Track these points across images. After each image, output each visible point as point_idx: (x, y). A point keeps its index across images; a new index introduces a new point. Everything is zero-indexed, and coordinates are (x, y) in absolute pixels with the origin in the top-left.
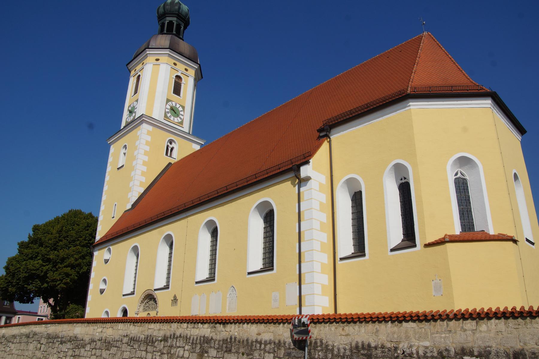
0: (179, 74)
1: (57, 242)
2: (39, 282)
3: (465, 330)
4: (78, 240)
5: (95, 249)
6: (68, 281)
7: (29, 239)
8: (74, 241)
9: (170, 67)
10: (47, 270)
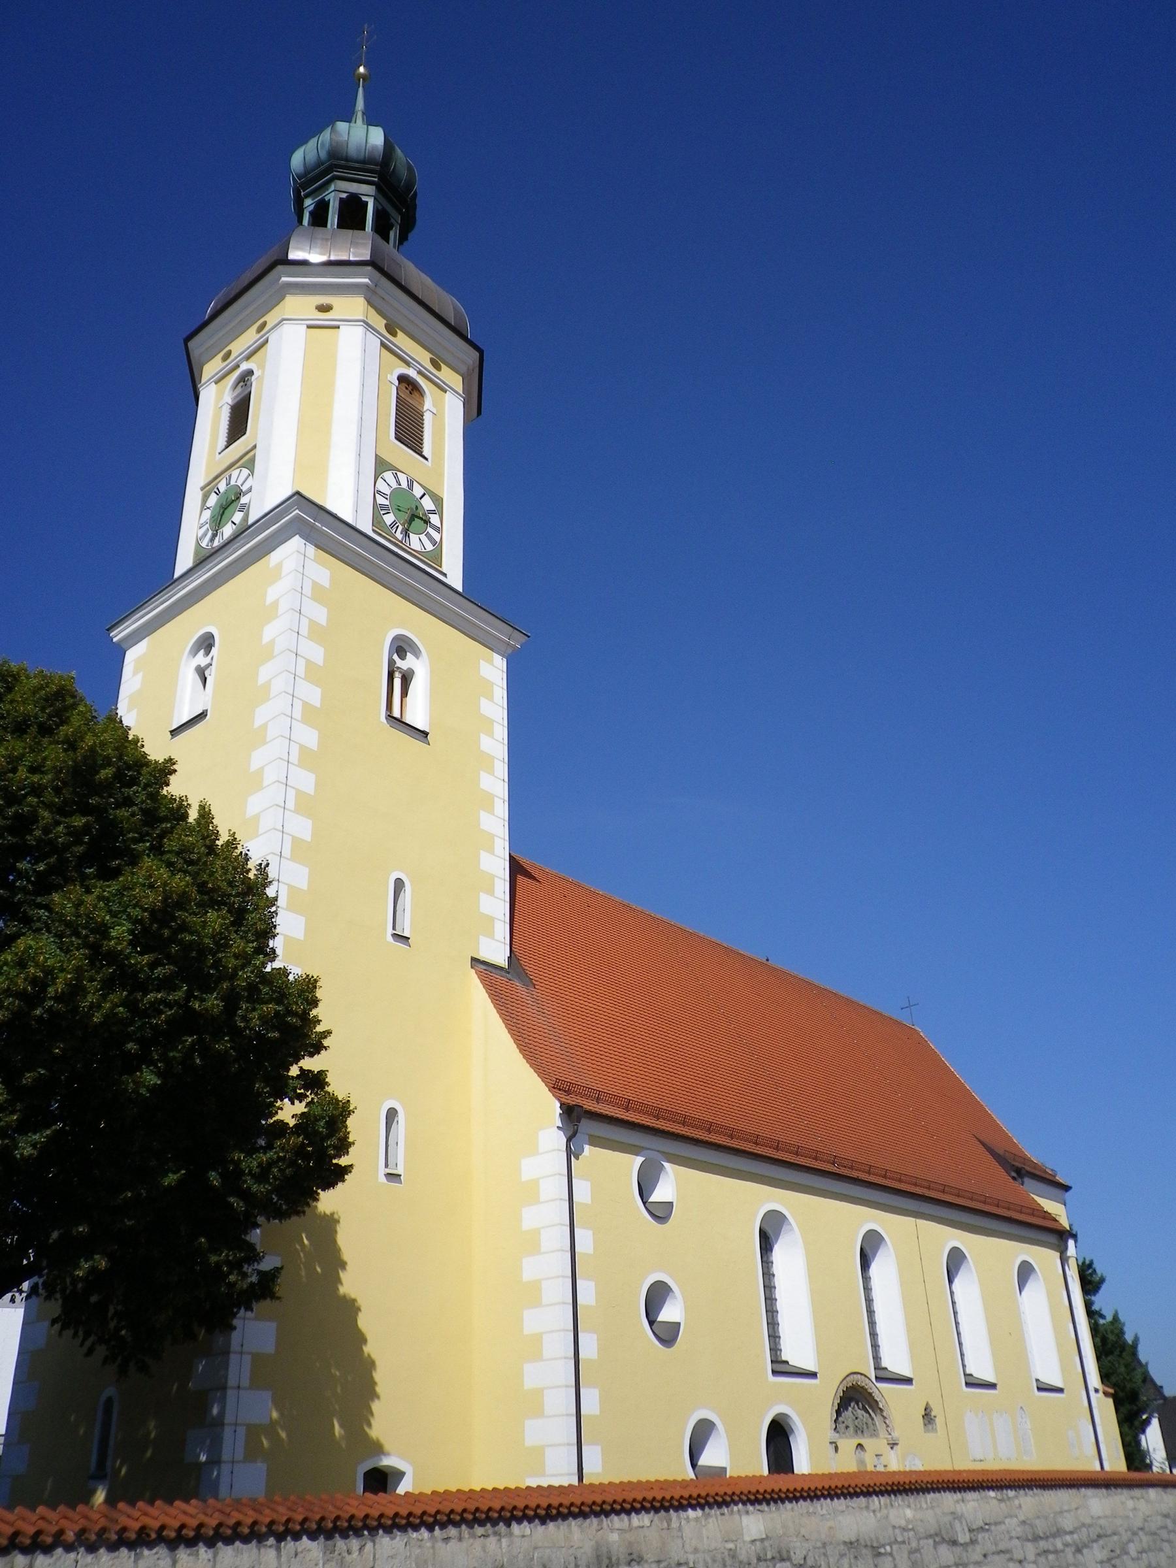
0: (412, 373)
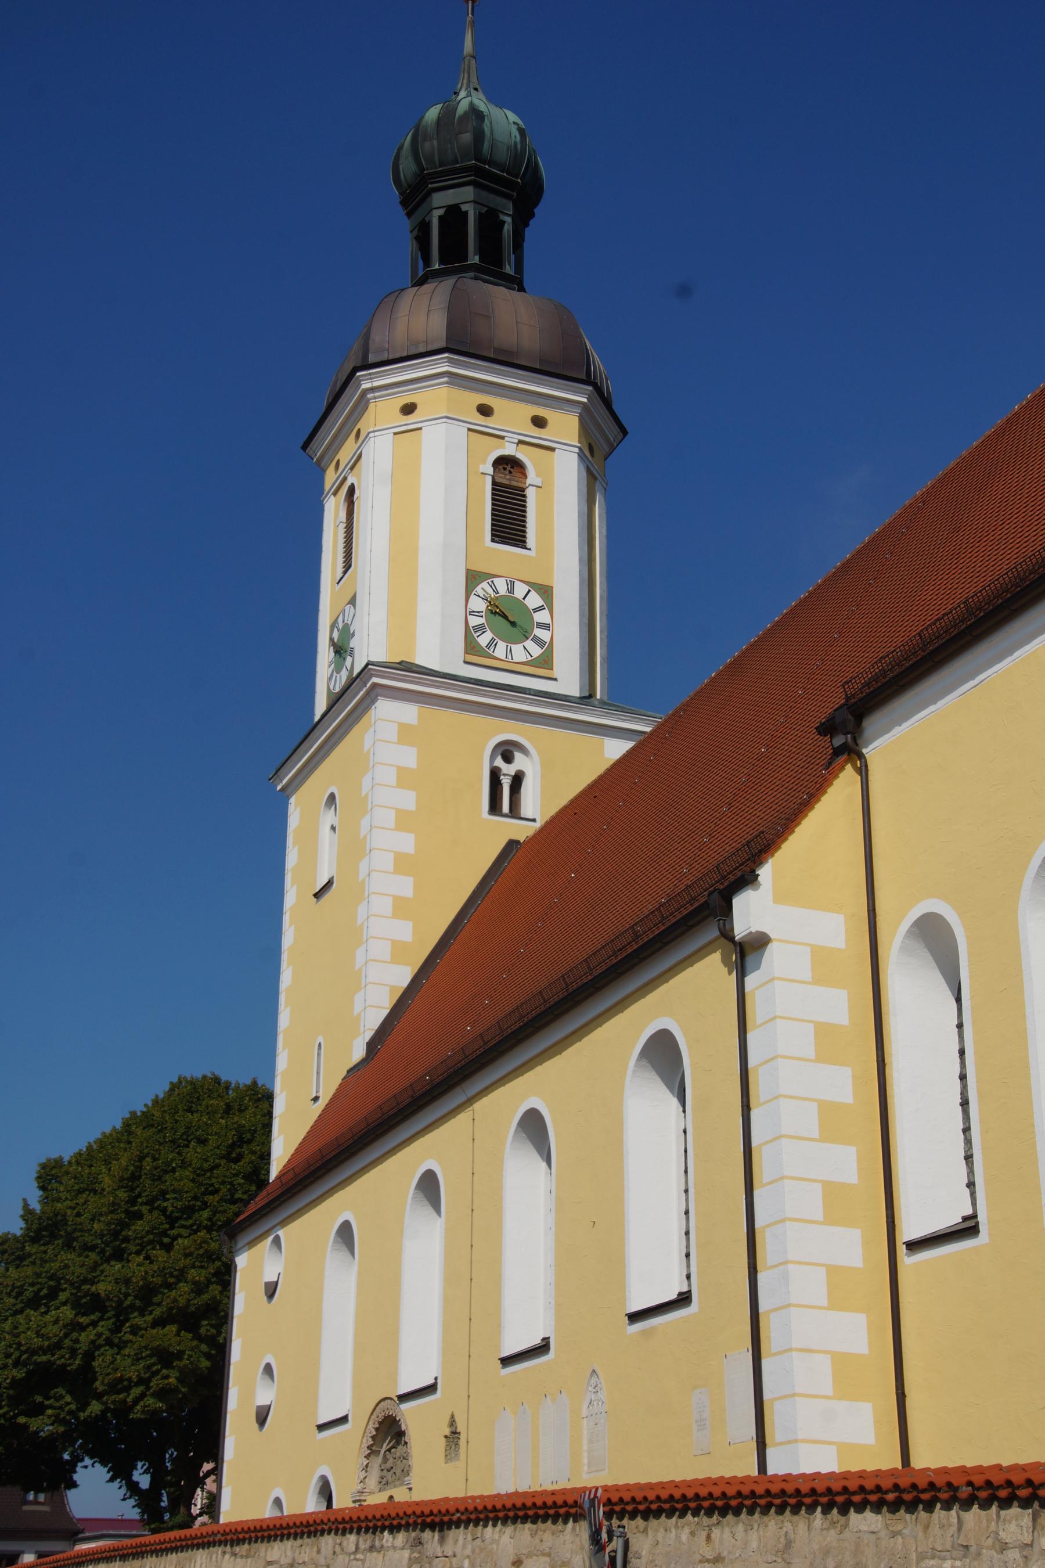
0: (509, 449)
1: (123, 1225)
2: (68, 1398)
3: (1004, 1547)
4: (205, 1205)
5: (240, 1244)
6: (171, 1380)
7: (26, 1221)
8: (189, 1211)
9: (462, 430)
10: (94, 1346)
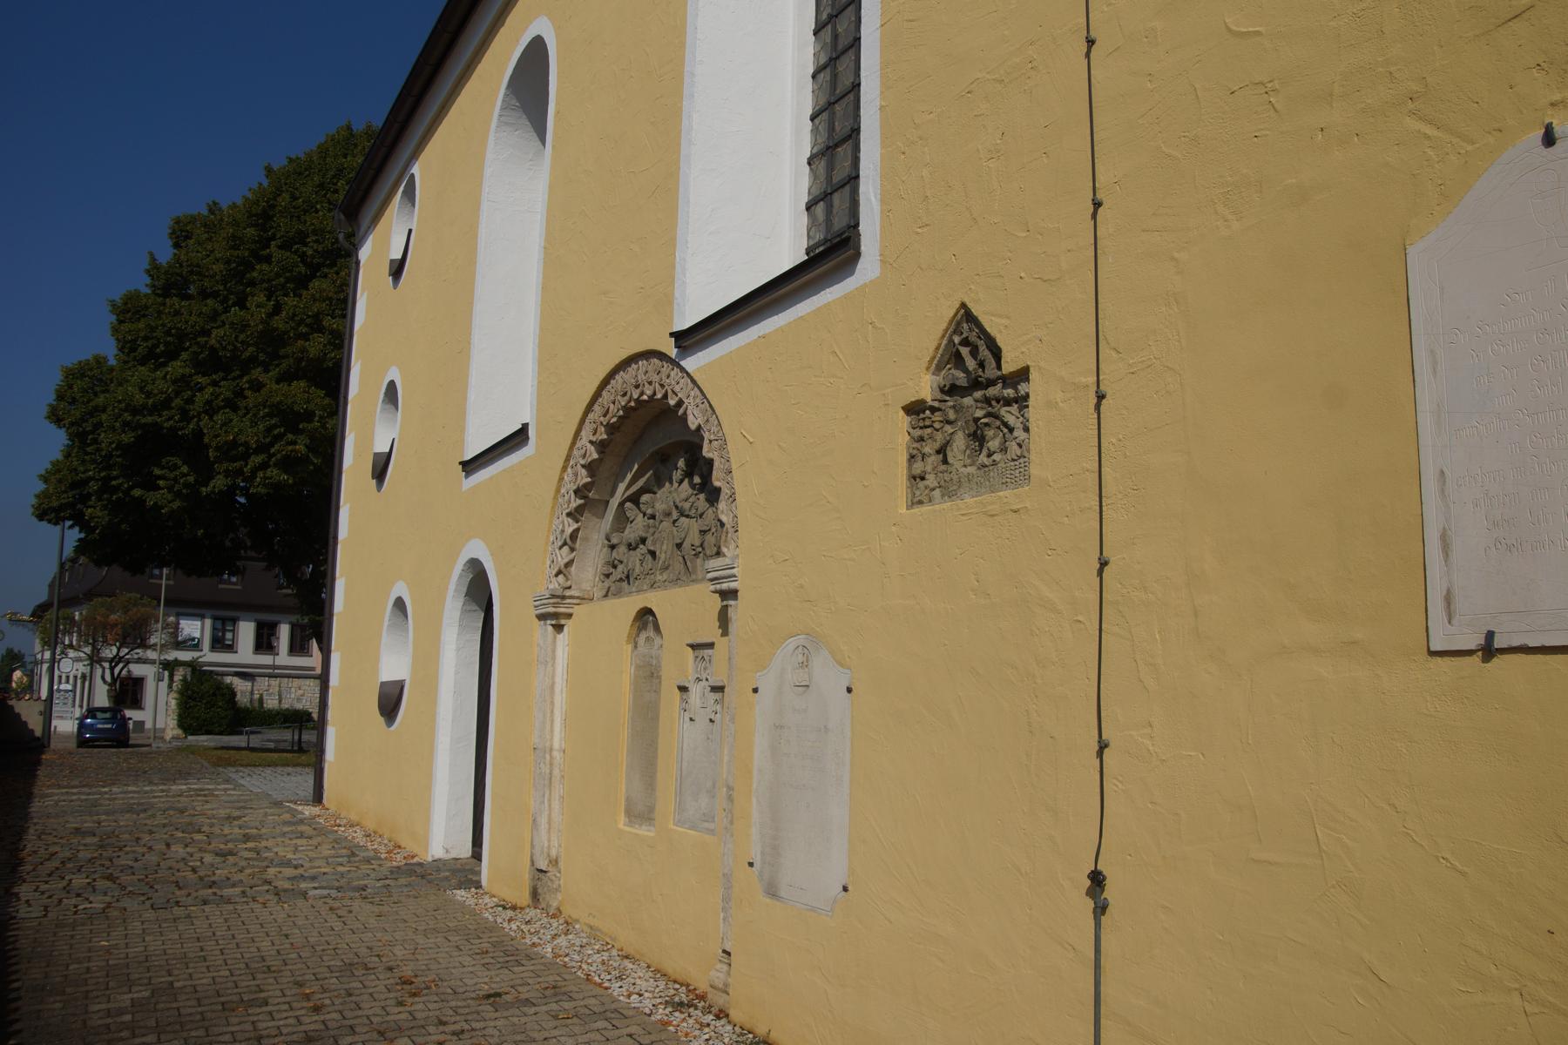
2: (185, 469)
6: (297, 447)
